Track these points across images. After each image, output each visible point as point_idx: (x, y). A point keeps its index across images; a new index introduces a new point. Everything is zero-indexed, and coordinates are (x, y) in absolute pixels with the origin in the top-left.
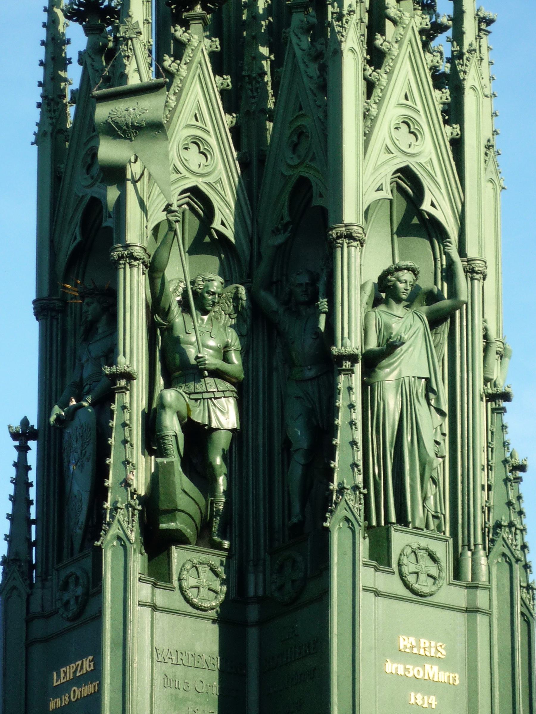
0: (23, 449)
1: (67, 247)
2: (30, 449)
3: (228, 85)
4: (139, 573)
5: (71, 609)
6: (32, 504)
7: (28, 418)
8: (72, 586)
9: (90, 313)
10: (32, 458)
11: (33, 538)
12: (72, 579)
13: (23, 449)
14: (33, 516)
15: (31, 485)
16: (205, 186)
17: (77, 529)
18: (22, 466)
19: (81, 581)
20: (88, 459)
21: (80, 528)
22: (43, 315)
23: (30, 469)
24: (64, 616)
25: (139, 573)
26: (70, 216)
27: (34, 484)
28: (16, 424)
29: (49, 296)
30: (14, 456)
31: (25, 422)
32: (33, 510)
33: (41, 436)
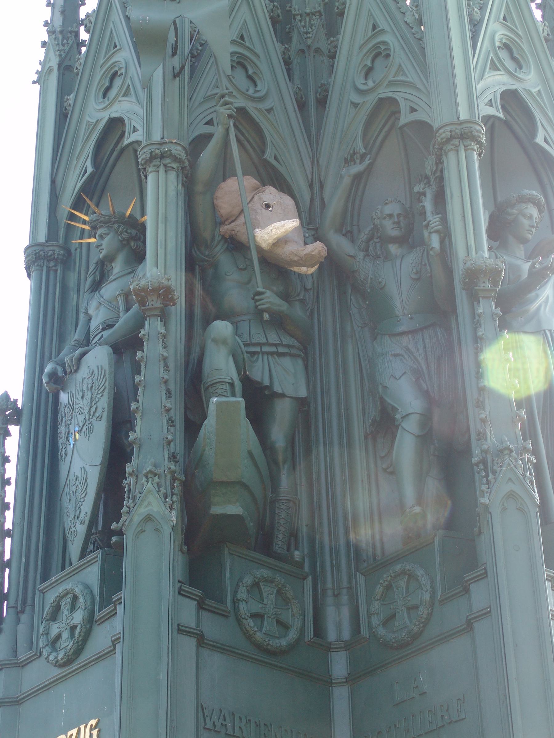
1: (73, 184)
2: (10, 435)
3: (278, 16)
4: (179, 581)
5: (62, 647)
6: (9, 509)
7: (9, 393)
8: (65, 612)
9: (103, 247)
11: (7, 556)
14: (8, 525)
15: (8, 482)
16: (256, 112)
17: (78, 525)
19: (81, 600)
20: (100, 418)
21: (82, 523)
22: (38, 265)
23: (9, 461)
24: (51, 658)
25: (179, 581)
27: (13, 481)
29: (47, 241)
32: (9, 515)
33: (25, 418)
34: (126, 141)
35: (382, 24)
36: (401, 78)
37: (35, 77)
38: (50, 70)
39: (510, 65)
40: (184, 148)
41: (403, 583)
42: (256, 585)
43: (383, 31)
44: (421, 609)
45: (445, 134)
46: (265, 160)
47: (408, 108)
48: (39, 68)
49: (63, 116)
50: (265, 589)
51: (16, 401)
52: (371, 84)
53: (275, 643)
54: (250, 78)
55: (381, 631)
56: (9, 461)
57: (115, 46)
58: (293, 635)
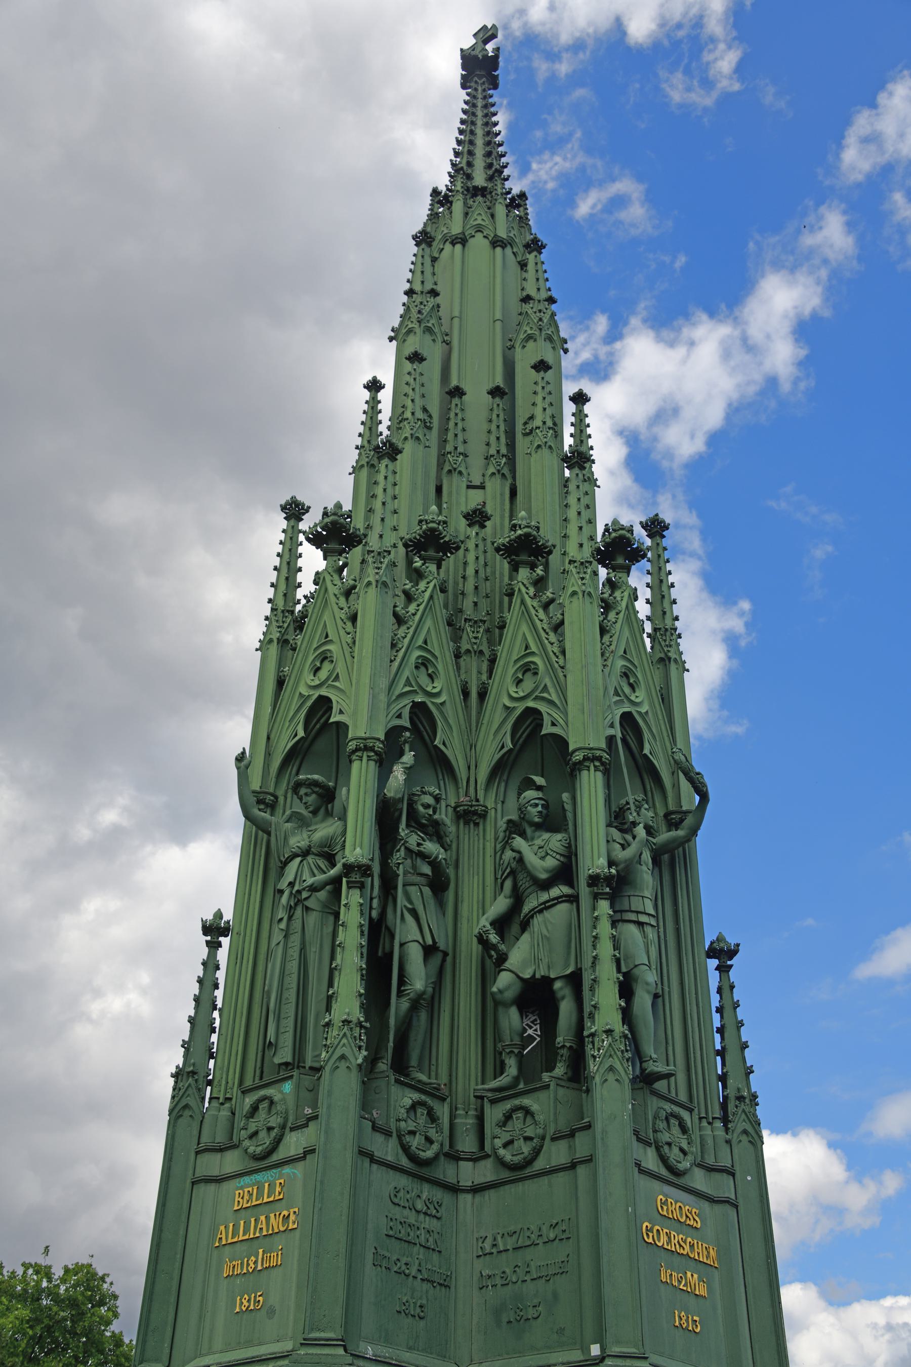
0: (213, 946)
1: (284, 744)
10: (223, 955)
12: (264, 1105)
13: (213, 946)
18: (210, 965)
26: (291, 713)
28: (209, 917)
30: (204, 952)
31: (219, 915)
34: (331, 720)
35: (534, 648)
36: (545, 695)
37: (258, 645)
38: (271, 641)
39: (627, 690)
40: (382, 742)
41: (520, 1115)
42: (413, 1107)
43: (533, 653)
44: (535, 1141)
45: (578, 756)
46: (436, 746)
47: (550, 723)
48: (262, 637)
49: (280, 683)
50: (419, 1111)
51: (228, 922)
52: (522, 694)
53: (423, 1155)
54: (430, 676)
55: (502, 1152)
56: (219, 969)
57: (327, 636)
58: (435, 1147)
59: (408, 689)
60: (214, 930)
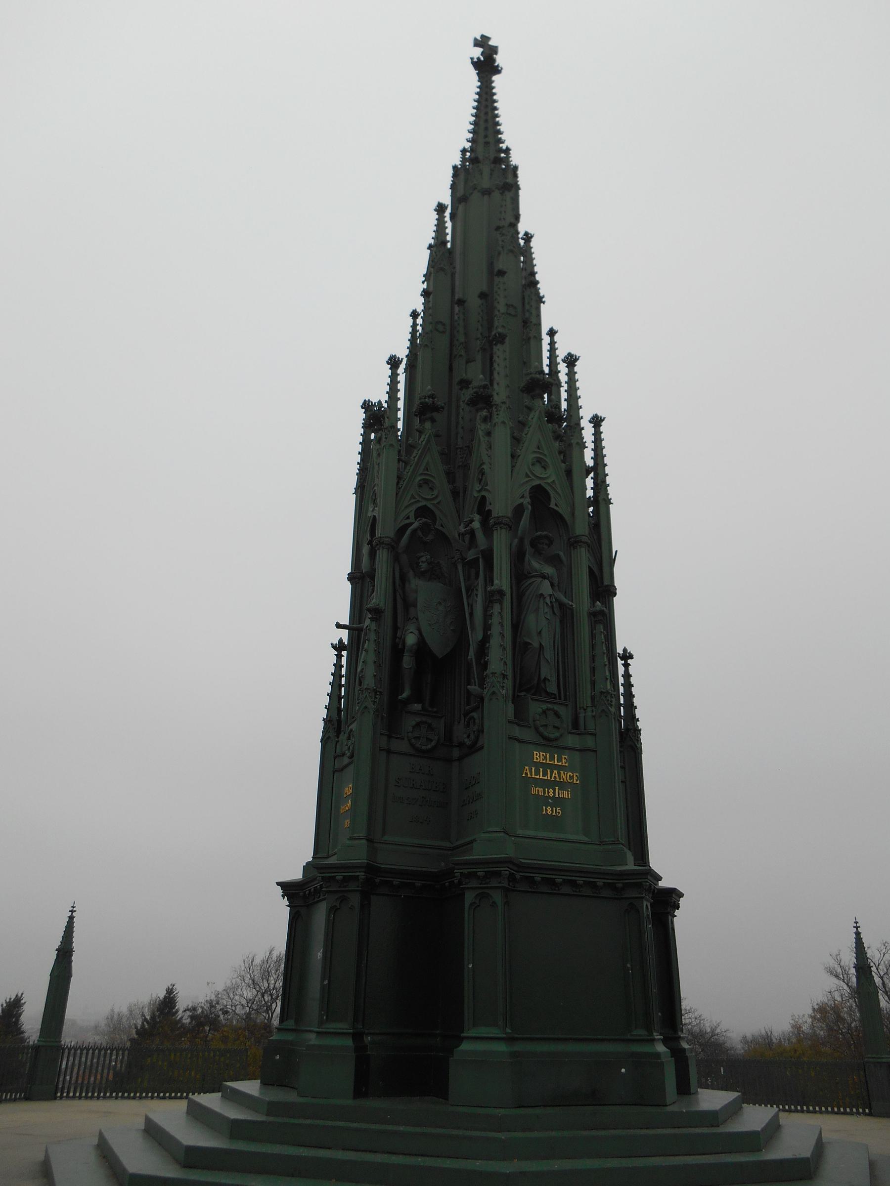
0: (339, 657)
10: (344, 661)
18: (338, 666)
28: (336, 642)
31: (341, 641)
42: (418, 725)
58: (433, 743)
59: (413, 501)
60: (339, 647)
